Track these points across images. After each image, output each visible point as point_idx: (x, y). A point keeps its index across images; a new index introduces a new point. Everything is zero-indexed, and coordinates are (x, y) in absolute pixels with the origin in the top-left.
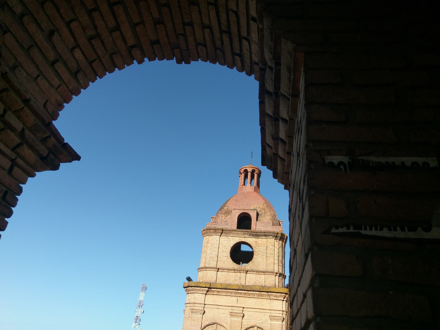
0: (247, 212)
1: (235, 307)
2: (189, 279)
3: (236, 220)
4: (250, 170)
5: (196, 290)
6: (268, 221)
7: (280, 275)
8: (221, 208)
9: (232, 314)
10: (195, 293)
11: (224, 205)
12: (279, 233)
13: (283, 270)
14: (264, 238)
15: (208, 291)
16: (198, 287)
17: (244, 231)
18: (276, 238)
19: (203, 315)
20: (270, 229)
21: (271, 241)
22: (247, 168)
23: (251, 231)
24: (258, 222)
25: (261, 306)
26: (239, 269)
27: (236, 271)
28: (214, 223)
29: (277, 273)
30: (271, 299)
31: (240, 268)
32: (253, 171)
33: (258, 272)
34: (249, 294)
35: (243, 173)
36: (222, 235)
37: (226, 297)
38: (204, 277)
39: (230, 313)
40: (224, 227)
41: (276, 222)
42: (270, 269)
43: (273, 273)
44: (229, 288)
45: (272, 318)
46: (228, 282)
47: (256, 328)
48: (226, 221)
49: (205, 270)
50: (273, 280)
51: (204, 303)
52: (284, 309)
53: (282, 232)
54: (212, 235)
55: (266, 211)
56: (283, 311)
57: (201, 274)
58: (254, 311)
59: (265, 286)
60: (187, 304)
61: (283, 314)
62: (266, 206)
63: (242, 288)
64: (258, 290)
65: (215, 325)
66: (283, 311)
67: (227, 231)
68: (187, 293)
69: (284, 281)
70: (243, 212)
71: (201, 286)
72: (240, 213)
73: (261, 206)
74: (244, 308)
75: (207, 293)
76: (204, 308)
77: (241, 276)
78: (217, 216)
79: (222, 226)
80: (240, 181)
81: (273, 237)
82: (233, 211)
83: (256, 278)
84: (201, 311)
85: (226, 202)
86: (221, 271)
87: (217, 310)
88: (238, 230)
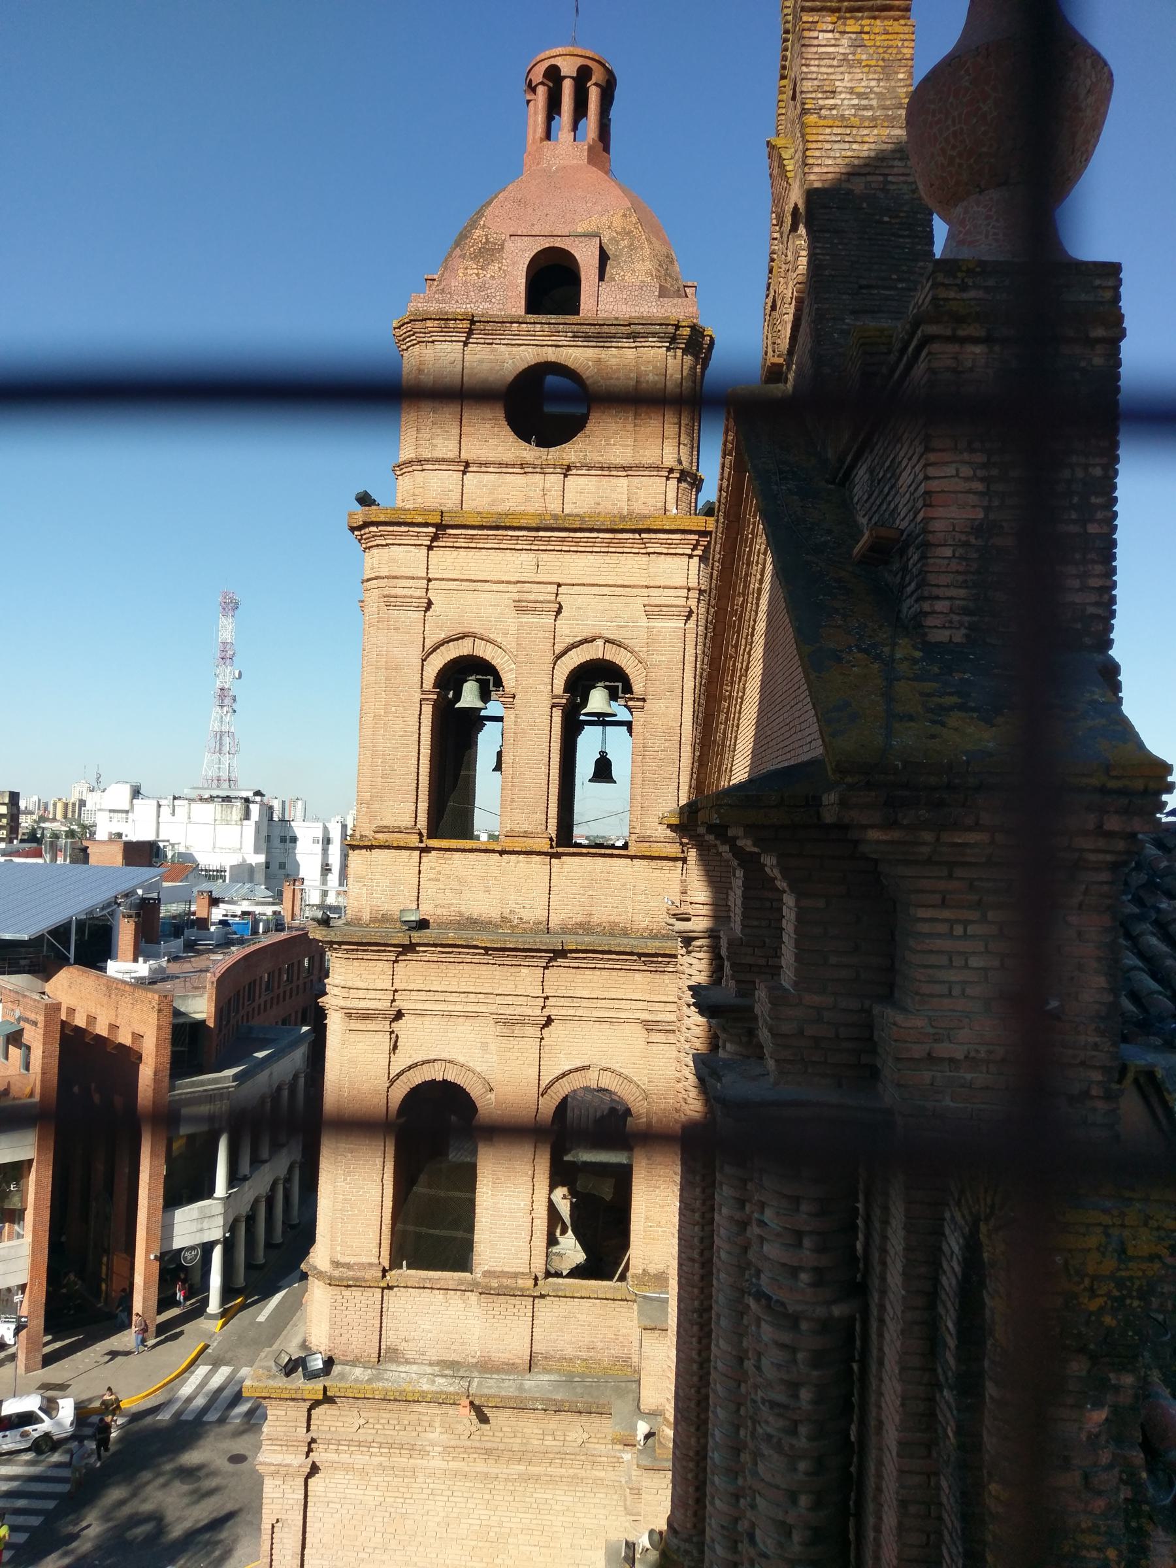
0: (563, 246)
1: (529, 582)
2: (365, 500)
3: (522, 282)
4: (568, 67)
5: (392, 533)
6: (642, 281)
7: (684, 476)
8: (463, 237)
9: (521, 607)
10: (393, 544)
11: (473, 224)
12: (684, 324)
13: (695, 458)
14: (627, 345)
15: (435, 538)
16: (399, 524)
17: (553, 321)
18: (671, 344)
19: (425, 612)
20: (652, 308)
22: (558, 62)
23: (579, 321)
24: (604, 286)
25: (616, 578)
26: (538, 462)
27: (530, 470)
28: (437, 296)
29: (671, 471)
30: (649, 554)
31: (545, 457)
32: (583, 75)
34: (577, 542)
35: (542, 83)
36: (471, 340)
37: (499, 553)
38: (417, 493)
39: (514, 601)
40: (478, 308)
41: (672, 286)
43: (658, 468)
44: (508, 524)
45: (652, 611)
46: (501, 508)
47: (600, 642)
48: (483, 288)
49: (419, 468)
50: (658, 494)
51: (425, 575)
52: (693, 583)
53: (695, 321)
54: (433, 342)
55: (636, 242)
56: (689, 589)
57: (405, 484)
58: (593, 592)
59: (630, 514)
60: (368, 580)
61: (687, 598)
62: (634, 220)
63: (552, 522)
64: (608, 525)
65: (468, 642)
66: (689, 589)
67: (488, 322)
68: (365, 548)
69: (697, 495)
70: (547, 245)
71: (410, 521)
72: (536, 251)
73: (618, 222)
74: (559, 585)
75: (433, 544)
76: (427, 589)
77: (548, 486)
78: (446, 269)
79: (468, 306)
80: (531, 122)
81: (661, 339)
82: (510, 245)
83: (599, 489)
84: (417, 600)
85: (477, 213)
86: (475, 469)
87: (470, 595)
88: (531, 318)
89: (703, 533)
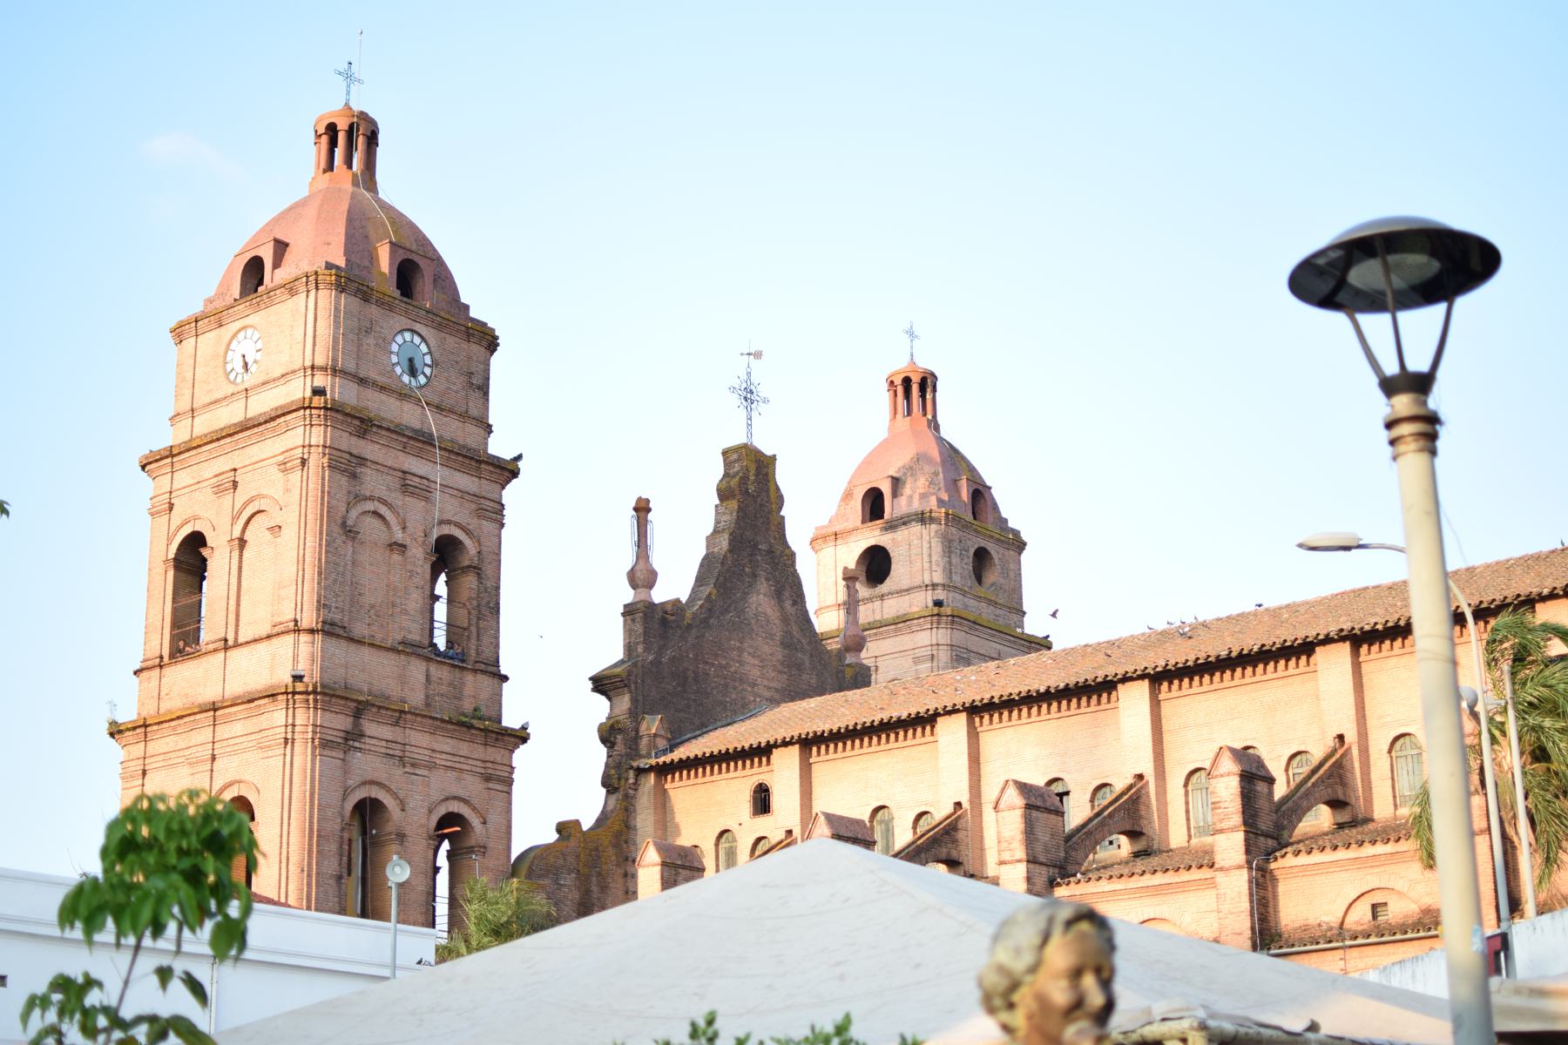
21: (916, 528)
33: (900, 592)
34: (881, 633)
42: (917, 582)
45: (917, 660)
74: (876, 657)
81: (917, 522)
89: (932, 616)
